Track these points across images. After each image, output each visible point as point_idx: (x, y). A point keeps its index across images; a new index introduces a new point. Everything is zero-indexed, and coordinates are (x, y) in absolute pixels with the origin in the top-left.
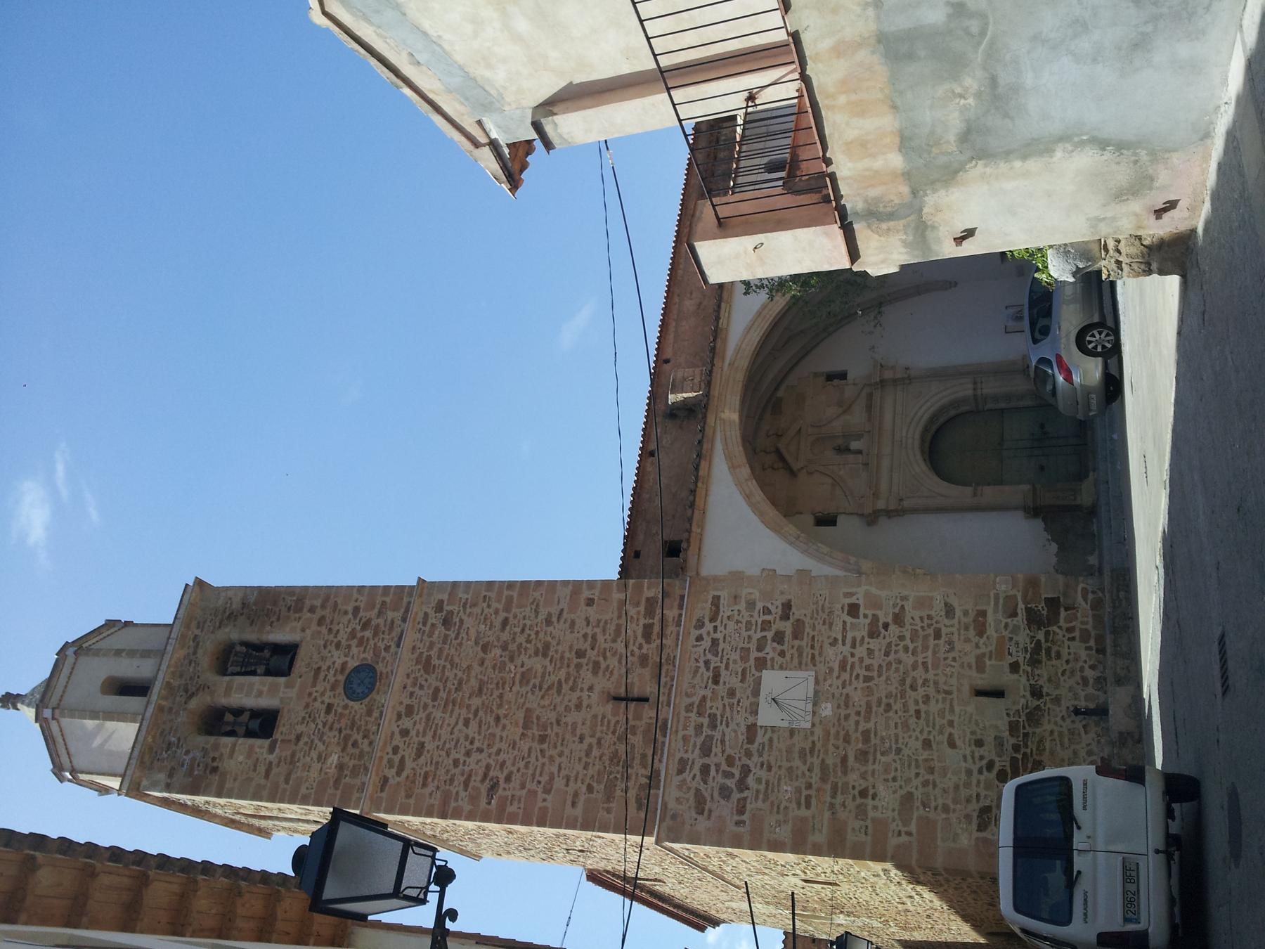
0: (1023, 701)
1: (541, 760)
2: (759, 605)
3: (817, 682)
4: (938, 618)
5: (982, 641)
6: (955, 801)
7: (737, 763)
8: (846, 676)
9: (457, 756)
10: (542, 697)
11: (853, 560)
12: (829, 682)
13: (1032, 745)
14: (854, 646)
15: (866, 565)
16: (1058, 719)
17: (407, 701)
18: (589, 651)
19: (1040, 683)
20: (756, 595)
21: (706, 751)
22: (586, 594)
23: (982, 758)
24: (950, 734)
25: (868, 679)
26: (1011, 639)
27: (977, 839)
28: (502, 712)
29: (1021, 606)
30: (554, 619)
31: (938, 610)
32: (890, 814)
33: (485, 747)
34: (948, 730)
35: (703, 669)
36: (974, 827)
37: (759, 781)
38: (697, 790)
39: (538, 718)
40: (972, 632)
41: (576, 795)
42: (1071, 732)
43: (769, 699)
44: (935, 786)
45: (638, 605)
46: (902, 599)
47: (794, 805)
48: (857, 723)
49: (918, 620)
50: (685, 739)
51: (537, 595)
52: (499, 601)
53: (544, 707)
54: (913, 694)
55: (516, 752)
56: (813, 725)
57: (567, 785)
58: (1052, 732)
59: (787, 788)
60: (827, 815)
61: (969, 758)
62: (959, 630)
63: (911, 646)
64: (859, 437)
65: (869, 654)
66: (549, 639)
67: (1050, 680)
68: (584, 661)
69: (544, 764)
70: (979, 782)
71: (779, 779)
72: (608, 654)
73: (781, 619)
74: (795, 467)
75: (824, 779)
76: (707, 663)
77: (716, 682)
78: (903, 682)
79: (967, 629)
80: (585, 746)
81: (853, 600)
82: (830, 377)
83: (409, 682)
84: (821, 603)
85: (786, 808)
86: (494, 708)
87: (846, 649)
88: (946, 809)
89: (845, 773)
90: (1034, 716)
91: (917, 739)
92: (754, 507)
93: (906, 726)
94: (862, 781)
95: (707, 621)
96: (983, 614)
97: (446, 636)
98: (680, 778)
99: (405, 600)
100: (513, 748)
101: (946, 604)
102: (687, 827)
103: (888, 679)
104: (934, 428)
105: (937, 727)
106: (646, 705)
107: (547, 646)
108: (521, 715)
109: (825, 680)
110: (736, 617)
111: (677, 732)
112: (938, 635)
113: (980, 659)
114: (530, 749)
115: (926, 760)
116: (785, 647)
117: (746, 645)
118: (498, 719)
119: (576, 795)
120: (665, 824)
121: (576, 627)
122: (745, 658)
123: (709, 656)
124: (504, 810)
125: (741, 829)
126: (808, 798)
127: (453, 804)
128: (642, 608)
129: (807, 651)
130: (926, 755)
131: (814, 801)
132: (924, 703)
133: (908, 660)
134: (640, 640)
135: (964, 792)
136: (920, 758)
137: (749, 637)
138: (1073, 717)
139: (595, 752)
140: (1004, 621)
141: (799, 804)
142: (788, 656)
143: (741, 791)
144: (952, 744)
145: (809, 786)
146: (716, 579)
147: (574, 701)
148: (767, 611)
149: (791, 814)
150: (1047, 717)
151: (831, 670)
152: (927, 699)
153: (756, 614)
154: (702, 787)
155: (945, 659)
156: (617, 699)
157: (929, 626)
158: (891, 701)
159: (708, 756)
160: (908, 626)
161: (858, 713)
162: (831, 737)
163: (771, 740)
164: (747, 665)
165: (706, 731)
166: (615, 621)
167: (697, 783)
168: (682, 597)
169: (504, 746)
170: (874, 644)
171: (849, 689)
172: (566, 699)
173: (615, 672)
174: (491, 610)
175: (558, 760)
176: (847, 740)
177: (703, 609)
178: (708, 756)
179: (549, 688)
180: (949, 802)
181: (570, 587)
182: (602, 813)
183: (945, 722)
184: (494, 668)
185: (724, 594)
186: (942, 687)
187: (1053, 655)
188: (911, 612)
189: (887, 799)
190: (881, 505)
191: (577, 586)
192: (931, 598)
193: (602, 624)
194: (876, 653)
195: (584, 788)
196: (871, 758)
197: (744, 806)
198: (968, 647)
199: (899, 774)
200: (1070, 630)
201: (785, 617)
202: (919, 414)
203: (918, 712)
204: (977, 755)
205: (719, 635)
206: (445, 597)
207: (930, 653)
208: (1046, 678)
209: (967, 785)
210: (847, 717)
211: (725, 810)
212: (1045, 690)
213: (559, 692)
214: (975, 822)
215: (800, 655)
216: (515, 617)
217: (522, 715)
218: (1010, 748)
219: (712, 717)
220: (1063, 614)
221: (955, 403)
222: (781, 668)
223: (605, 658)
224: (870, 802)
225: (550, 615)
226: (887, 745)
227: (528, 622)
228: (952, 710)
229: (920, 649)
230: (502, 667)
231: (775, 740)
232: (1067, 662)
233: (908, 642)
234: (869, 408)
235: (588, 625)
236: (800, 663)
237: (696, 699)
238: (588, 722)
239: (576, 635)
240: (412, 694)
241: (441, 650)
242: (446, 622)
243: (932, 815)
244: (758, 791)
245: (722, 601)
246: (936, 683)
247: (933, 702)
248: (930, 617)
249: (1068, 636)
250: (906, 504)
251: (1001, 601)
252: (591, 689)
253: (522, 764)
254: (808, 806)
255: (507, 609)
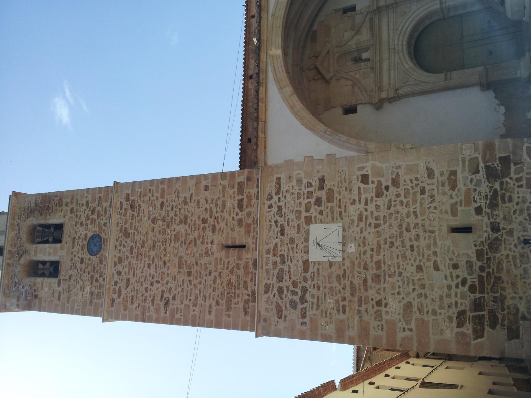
0: (485, 235)
1: (190, 287)
2: (305, 181)
3: (344, 230)
4: (423, 179)
5: (454, 193)
6: (441, 307)
7: (299, 285)
8: (362, 225)
9: (146, 286)
10: (187, 249)
11: (362, 143)
12: (352, 230)
13: (493, 266)
14: (366, 204)
15: (371, 146)
16: (512, 246)
17: (118, 255)
18: (209, 219)
19: (498, 220)
20: (302, 174)
21: (280, 279)
22: (204, 183)
23: (458, 277)
24: (435, 261)
25: (377, 226)
26: (475, 190)
27: (457, 333)
28: (166, 259)
29: (482, 165)
30: (188, 200)
31: (422, 173)
32: (397, 317)
33: (160, 280)
34: (434, 258)
35: (274, 226)
36: (454, 324)
37: (313, 296)
38: (277, 303)
39: (186, 261)
40: (447, 188)
41: (210, 307)
42: (522, 255)
43: (315, 243)
44: (426, 297)
45: (233, 187)
46: (398, 167)
47: (335, 312)
48: (372, 256)
49: (408, 182)
50: (267, 271)
51: (177, 186)
52: (157, 192)
53: (188, 255)
54: (408, 234)
55: (176, 282)
56: (344, 259)
57: (205, 301)
58: (508, 256)
59: (330, 301)
60: (357, 318)
61: (449, 277)
62: (438, 187)
63: (405, 201)
64: (366, 49)
65: (377, 209)
66: (186, 213)
67: (504, 218)
68: (207, 225)
69: (191, 289)
70: (456, 294)
71: (325, 295)
72: (220, 220)
73: (319, 189)
74: (327, 78)
75: (353, 294)
76: (276, 222)
77: (282, 234)
78: (401, 226)
79: (443, 185)
80: (212, 277)
81: (364, 172)
82: (345, 11)
83: (118, 243)
84: (343, 176)
85: (330, 313)
86: (162, 256)
87: (362, 206)
88: (434, 313)
89: (366, 290)
90: (494, 245)
91: (412, 265)
92: (296, 114)
93: (404, 256)
94: (377, 295)
95: (274, 194)
96: (454, 173)
97: (133, 215)
98: (267, 296)
99: (110, 195)
100: (175, 280)
101: (428, 169)
102: (273, 327)
103: (390, 225)
104: (416, 35)
105: (426, 257)
106: (244, 250)
107: (186, 217)
108: (176, 260)
109: (349, 228)
110: (291, 191)
111: (262, 267)
112: (423, 192)
113: (453, 207)
114: (183, 280)
115: (419, 280)
116: (322, 208)
117: (299, 209)
118: (165, 263)
119: (210, 307)
120: (260, 325)
121: (201, 204)
122: (298, 218)
123: (277, 218)
124: (174, 317)
125: (304, 328)
126: (344, 307)
127: (147, 314)
128: (236, 189)
129: (337, 209)
130: (419, 276)
131: (347, 309)
132: (416, 240)
133: (404, 210)
134: (237, 210)
135: (446, 301)
136: (415, 279)
137: (300, 203)
138: (523, 245)
139: (218, 281)
140: (470, 177)
141: (338, 311)
142: (325, 214)
143: (302, 303)
144: (436, 268)
145: (344, 299)
146: (277, 166)
147: (204, 250)
148: (310, 185)
149: (334, 318)
150: (503, 246)
151: (353, 221)
152: (418, 237)
153: (303, 188)
154: (280, 301)
155: (429, 208)
156: (228, 247)
157: (417, 185)
158: (394, 240)
159: (282, 281)
160: (402, 187)
161: (372, 250)
162: (356, 266)
163: (318, 270)
164: (300, 222)
165: (279, 266)
166: (221, 200)
167: (277, 299)
168: (258, 179)
169: (169, 279)
170: (380, 201)
171: (365, 234)
172: (200, 249)
173: (225, 231)
174: (154, 198)
175: (199, 286)
176: (366, 268)
177: (271, 187)
178: (282, 281)
179: (190, 243)
180: (436, 308)
181: (195, 180)
182: (225, 318)
183: (431, 252)
184: (160, 233)
185: (283, 176)
186: (428, 228)
187: (507, 199)
188: (404, 177)
189: (394, 307)
190: (384, 95)
191: (198, 178)
192: (417, 165)
193: (214, 201)
194: (382, 208)
195: (214, 303)
196: (382, 278)
197: (305, 313)
198: (445, 199)
199: (401, 290)
200: (519, 180)
201: (321, 188)
202: (405, 27)
203: (412, 247)
204: (454, 275)
205: (282, 204)
206: (129, 192)
207: (418, 205)
208: (502, 216)
209: (449, 296)
210: (365, 253)
211: (294, 315)
212: (501, 226)
213: (195, 245)
214: (455, 321)
215: (332, 212)
216: (167, 201)
217: (177, 260)
218: (478, 269)
219: (282, 256)
220: (513, 168)
221: (429, 16)
222: (321, 222)
223: (218, 223)
224: (383, 309)
225: (185, 198)
226: (393, 270)
227: (174, 204)
228: (435, 243)
229: (411, 202)
230: (164, 232)
231: (321, 270)
232: (517, 204)
233: (402, 198)
234: (372, 27)
235: (207, 202)
236: (333, 218)
237: (272, 246)
238: (213, 263)
239: (201, 209)
240: (120, 250)
241: (131, 224)
242: (132, 207)
243: (425, 317)
244: (313, 303)
245: (282, 181)
246: (423, 226)
247: (421, 239)
248: (417, 179)
249: (517, 184)
250: (400, 92)
251: (467, 163)
252: (212, 242)
253: (180, 289)
254: (344, 312)
255: (162, 197)
